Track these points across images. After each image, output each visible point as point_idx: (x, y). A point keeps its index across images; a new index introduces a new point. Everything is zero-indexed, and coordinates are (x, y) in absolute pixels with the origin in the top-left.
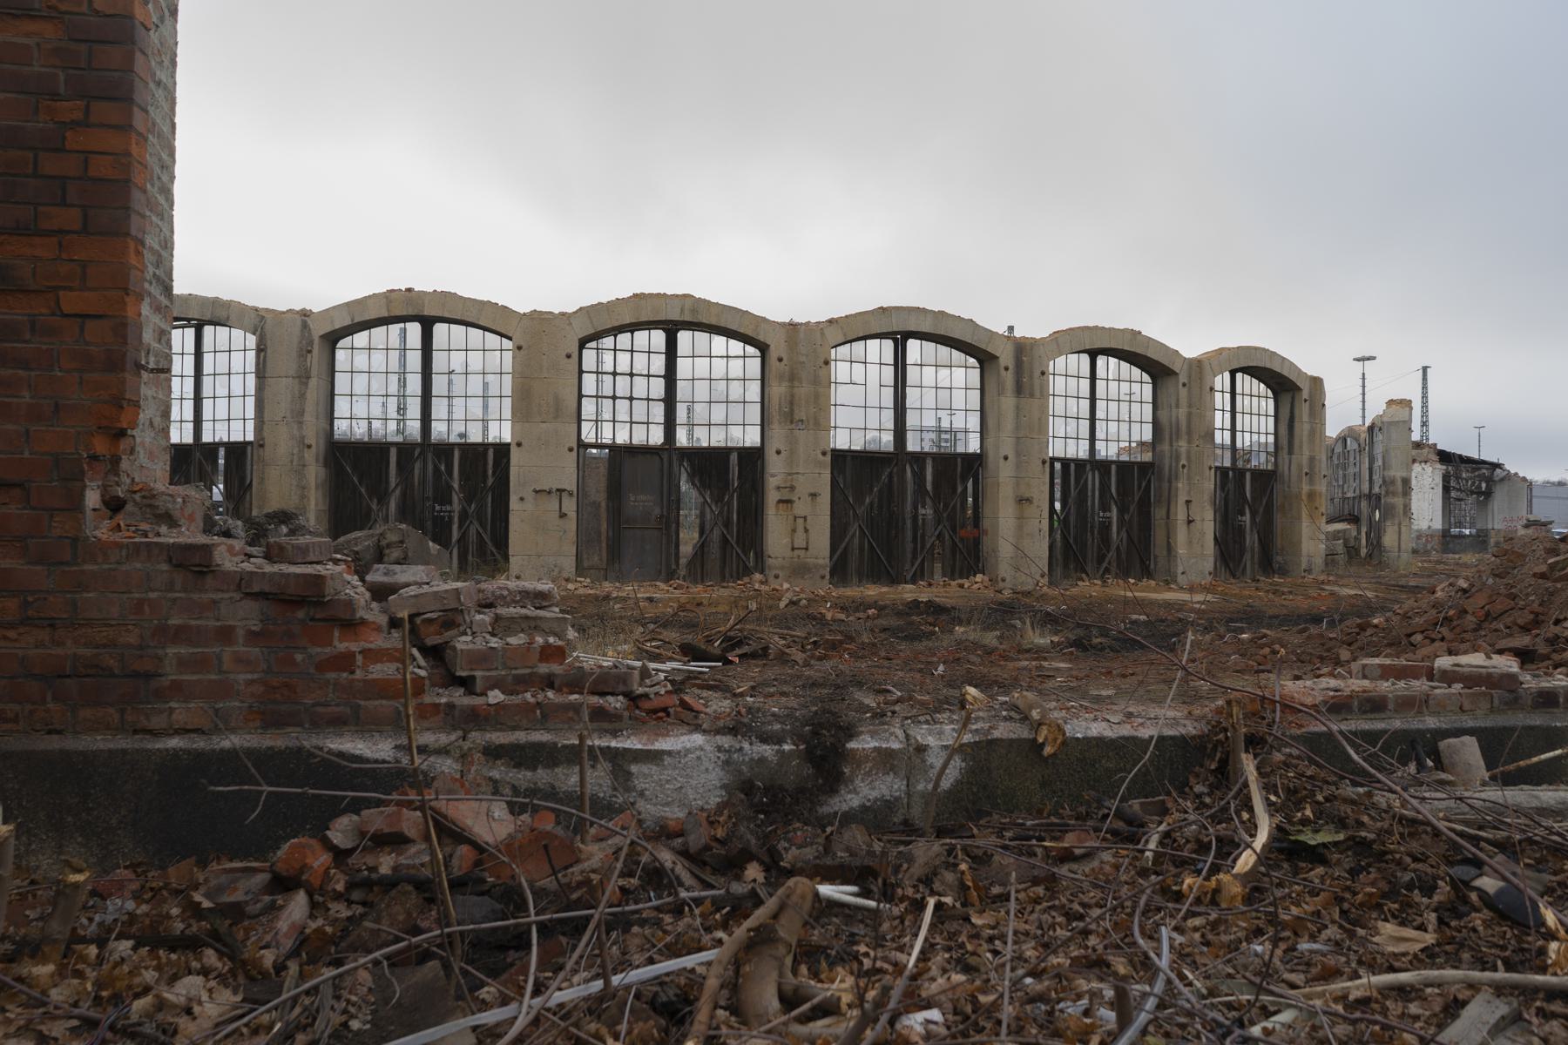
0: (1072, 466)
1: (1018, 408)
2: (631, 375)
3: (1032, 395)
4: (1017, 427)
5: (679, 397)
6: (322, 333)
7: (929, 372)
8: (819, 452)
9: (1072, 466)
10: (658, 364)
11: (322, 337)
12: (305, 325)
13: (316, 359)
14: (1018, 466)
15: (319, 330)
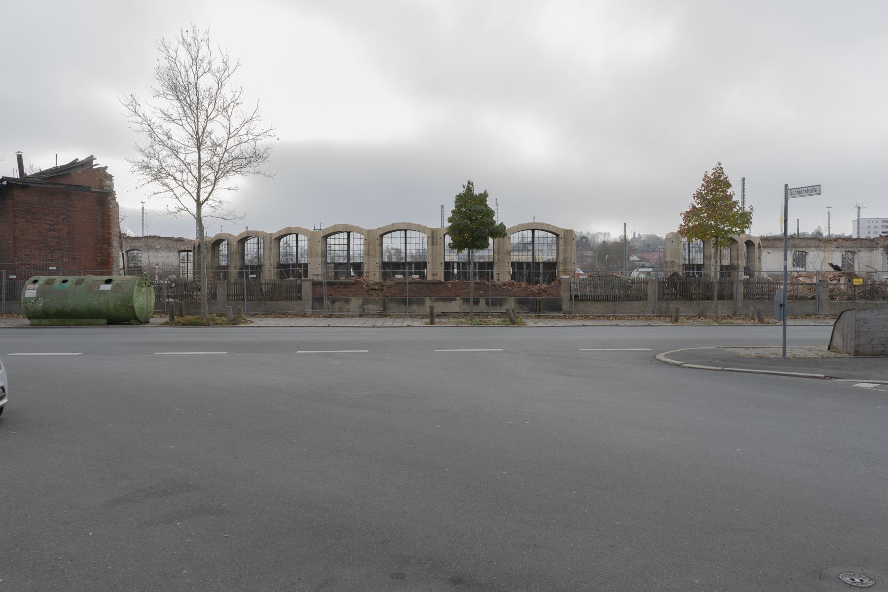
0: (461, 264)
1: (432, 248)
2: (339, 244)
3: (437, 245)
4: (432, 254)
5: (351, 250)
6: (275, 238)
7: (413, 239)
8: (375, 263)
9: (461, 264)
10: (346, 241)
11: (275, 239)
12: (271, 237)
13: (274, 245)
14: (433, 265)
15: (274, 237)
